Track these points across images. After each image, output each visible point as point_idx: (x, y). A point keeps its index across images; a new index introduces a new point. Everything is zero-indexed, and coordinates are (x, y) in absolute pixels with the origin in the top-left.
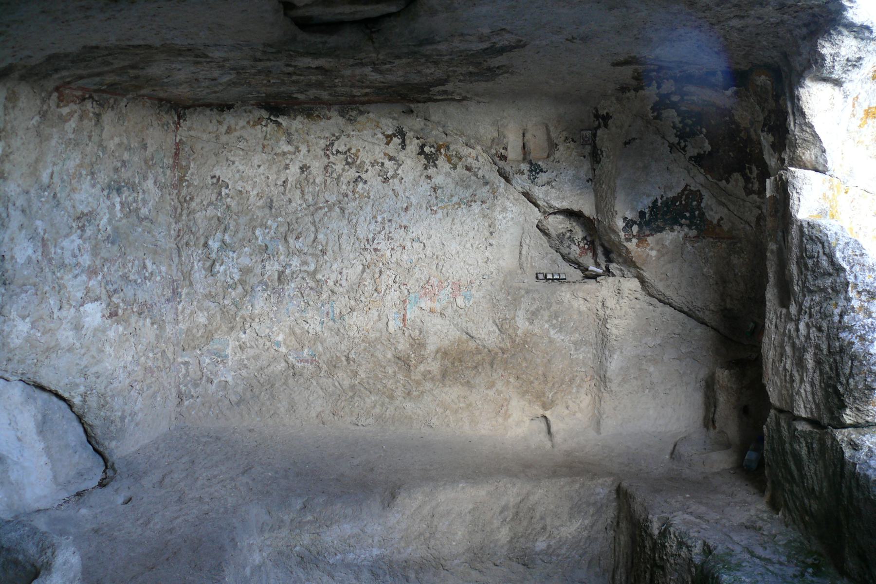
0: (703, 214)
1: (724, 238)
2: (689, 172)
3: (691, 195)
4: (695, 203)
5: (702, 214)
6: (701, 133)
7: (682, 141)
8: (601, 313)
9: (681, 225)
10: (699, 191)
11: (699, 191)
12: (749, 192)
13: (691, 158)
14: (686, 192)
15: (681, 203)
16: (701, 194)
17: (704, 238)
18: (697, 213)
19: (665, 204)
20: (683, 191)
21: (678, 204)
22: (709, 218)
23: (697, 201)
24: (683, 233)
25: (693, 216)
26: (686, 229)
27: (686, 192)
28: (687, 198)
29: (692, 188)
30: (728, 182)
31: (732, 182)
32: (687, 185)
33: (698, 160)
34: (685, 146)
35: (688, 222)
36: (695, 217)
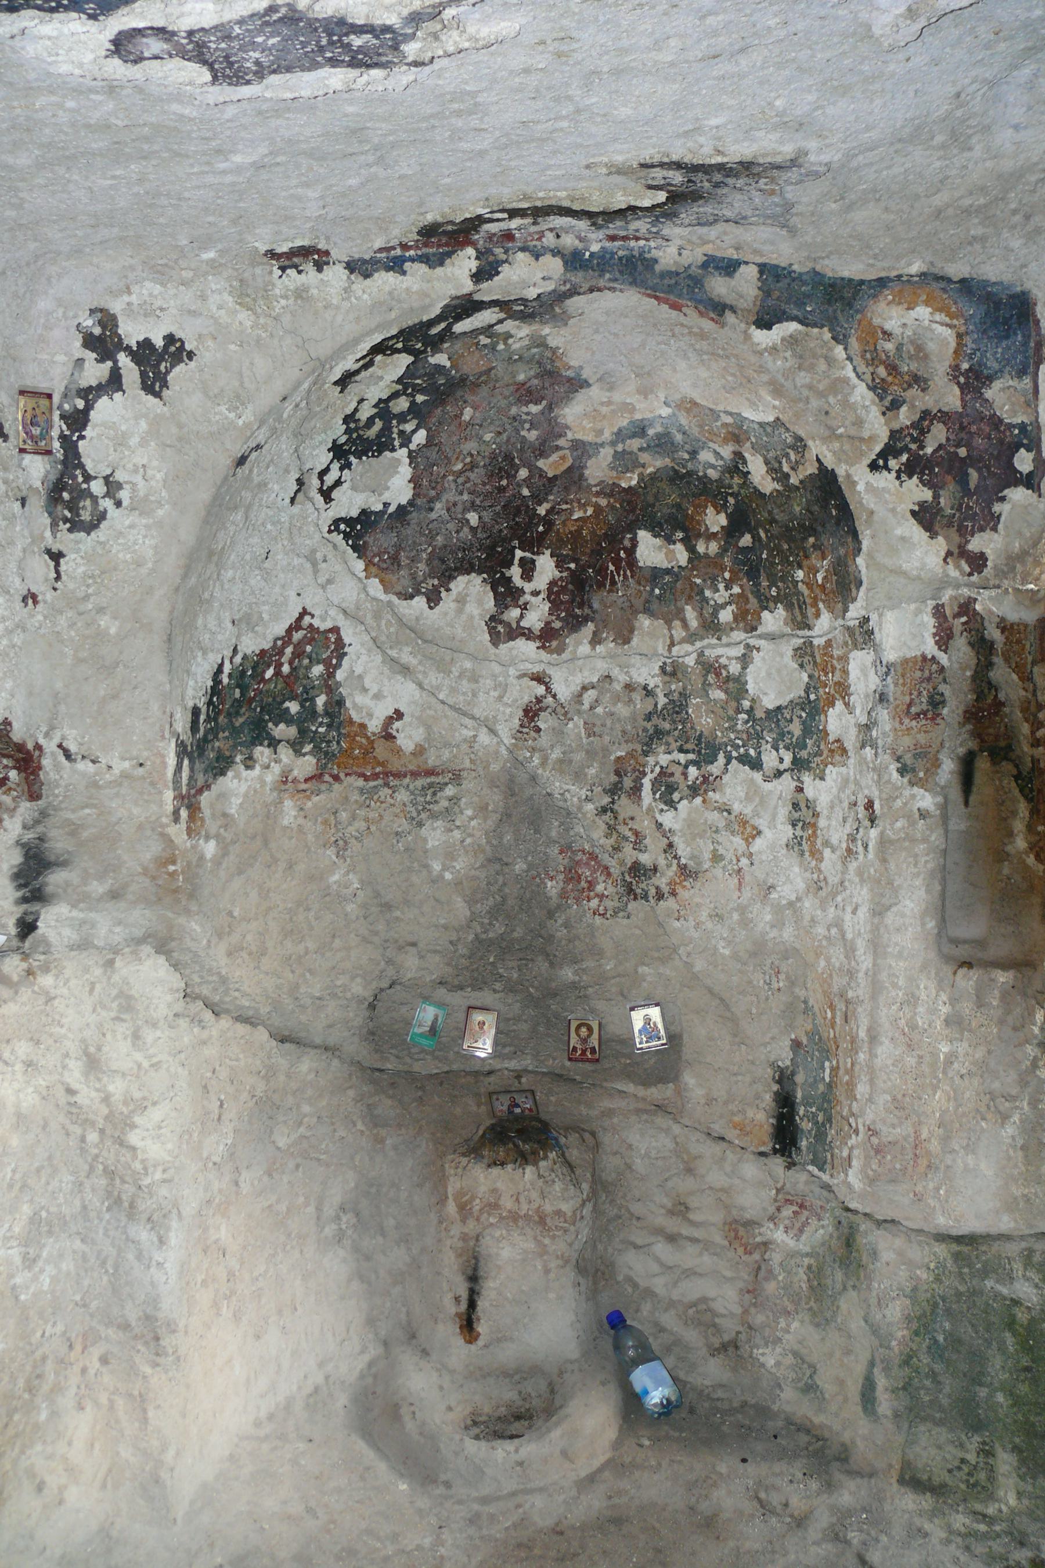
0: (340, 703)
1: (398, 775)
2: (316, 572)
3: (314, 644)
4: (318, 670)
5: (337, 704)
6: (406, 439)
7: (336, 466)
8: (87, 1096)
9: (274, 743)
10: (335, 630)
11: (335, 630)
12: (501, 631)
13: (337, 522)
14: (297, 636)
15: (278, 673)
16: (340, 643)
17: (336, 778)
18: (321, 701)
19: (239, 676)
20: (290, 631)
21: (269, 673)
22: (355, 717)
23: (327, 663)
24: (276, 769)
25: (310, 713)
26: (285, 754)
27: (297, 636)
28: (298, 654)
29: (316, 622)
30: (434, 599)
31: (448, 602)
32: (304, 612)
33: (357, 530)
34: (338, 483)
35: (292, 731)
36: (314, 714)
